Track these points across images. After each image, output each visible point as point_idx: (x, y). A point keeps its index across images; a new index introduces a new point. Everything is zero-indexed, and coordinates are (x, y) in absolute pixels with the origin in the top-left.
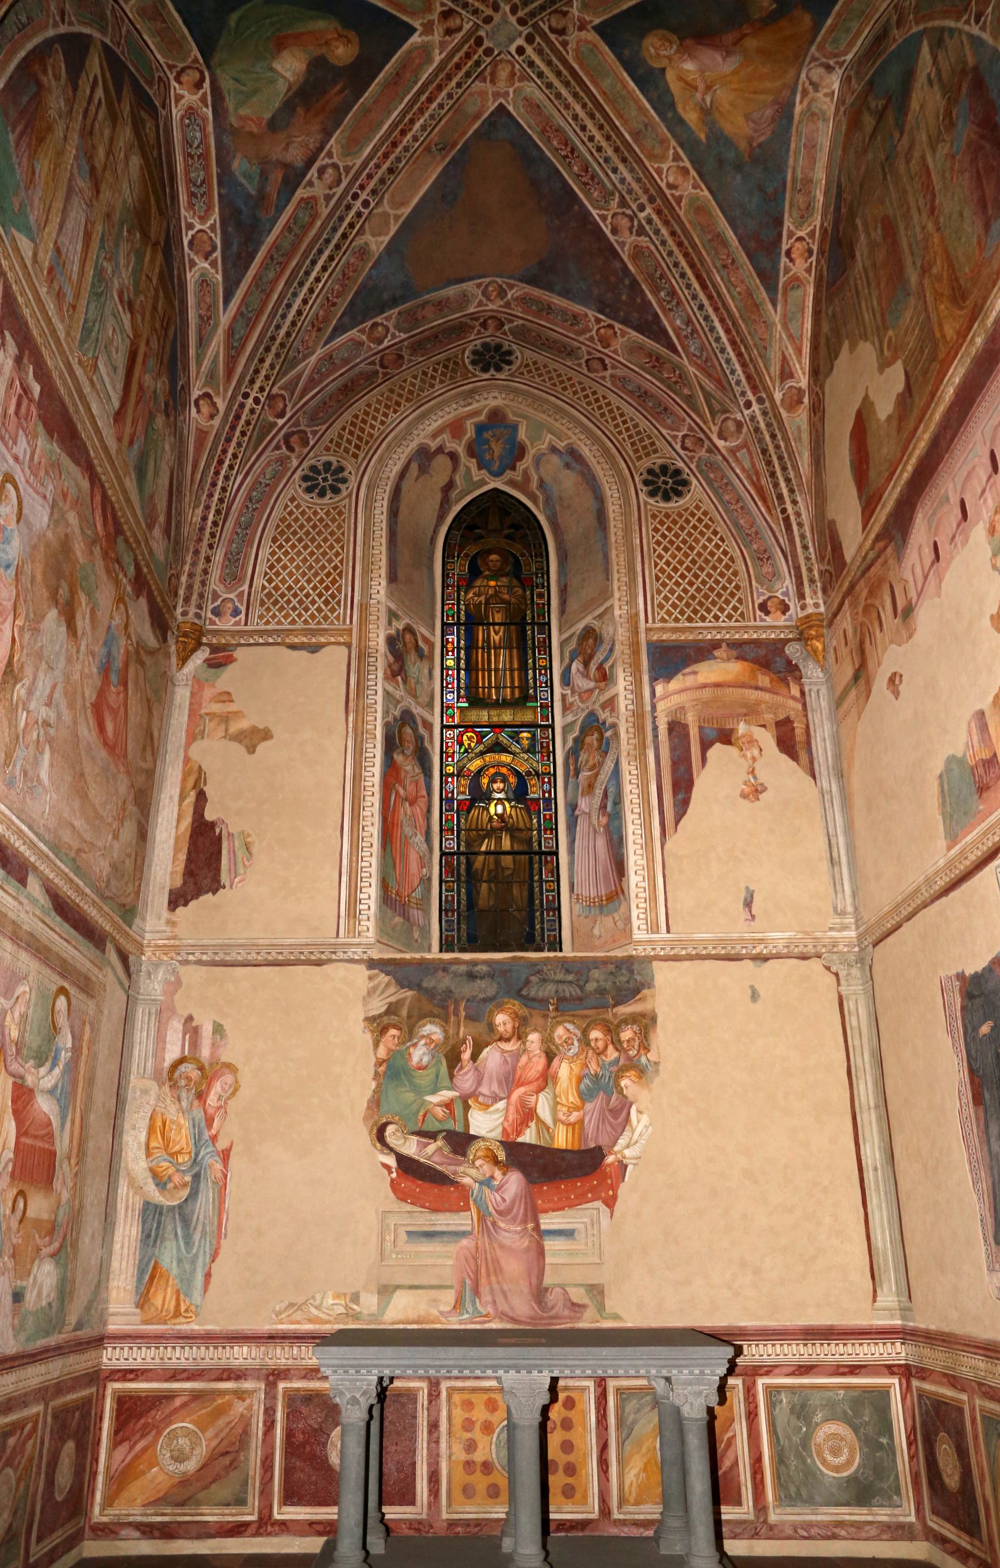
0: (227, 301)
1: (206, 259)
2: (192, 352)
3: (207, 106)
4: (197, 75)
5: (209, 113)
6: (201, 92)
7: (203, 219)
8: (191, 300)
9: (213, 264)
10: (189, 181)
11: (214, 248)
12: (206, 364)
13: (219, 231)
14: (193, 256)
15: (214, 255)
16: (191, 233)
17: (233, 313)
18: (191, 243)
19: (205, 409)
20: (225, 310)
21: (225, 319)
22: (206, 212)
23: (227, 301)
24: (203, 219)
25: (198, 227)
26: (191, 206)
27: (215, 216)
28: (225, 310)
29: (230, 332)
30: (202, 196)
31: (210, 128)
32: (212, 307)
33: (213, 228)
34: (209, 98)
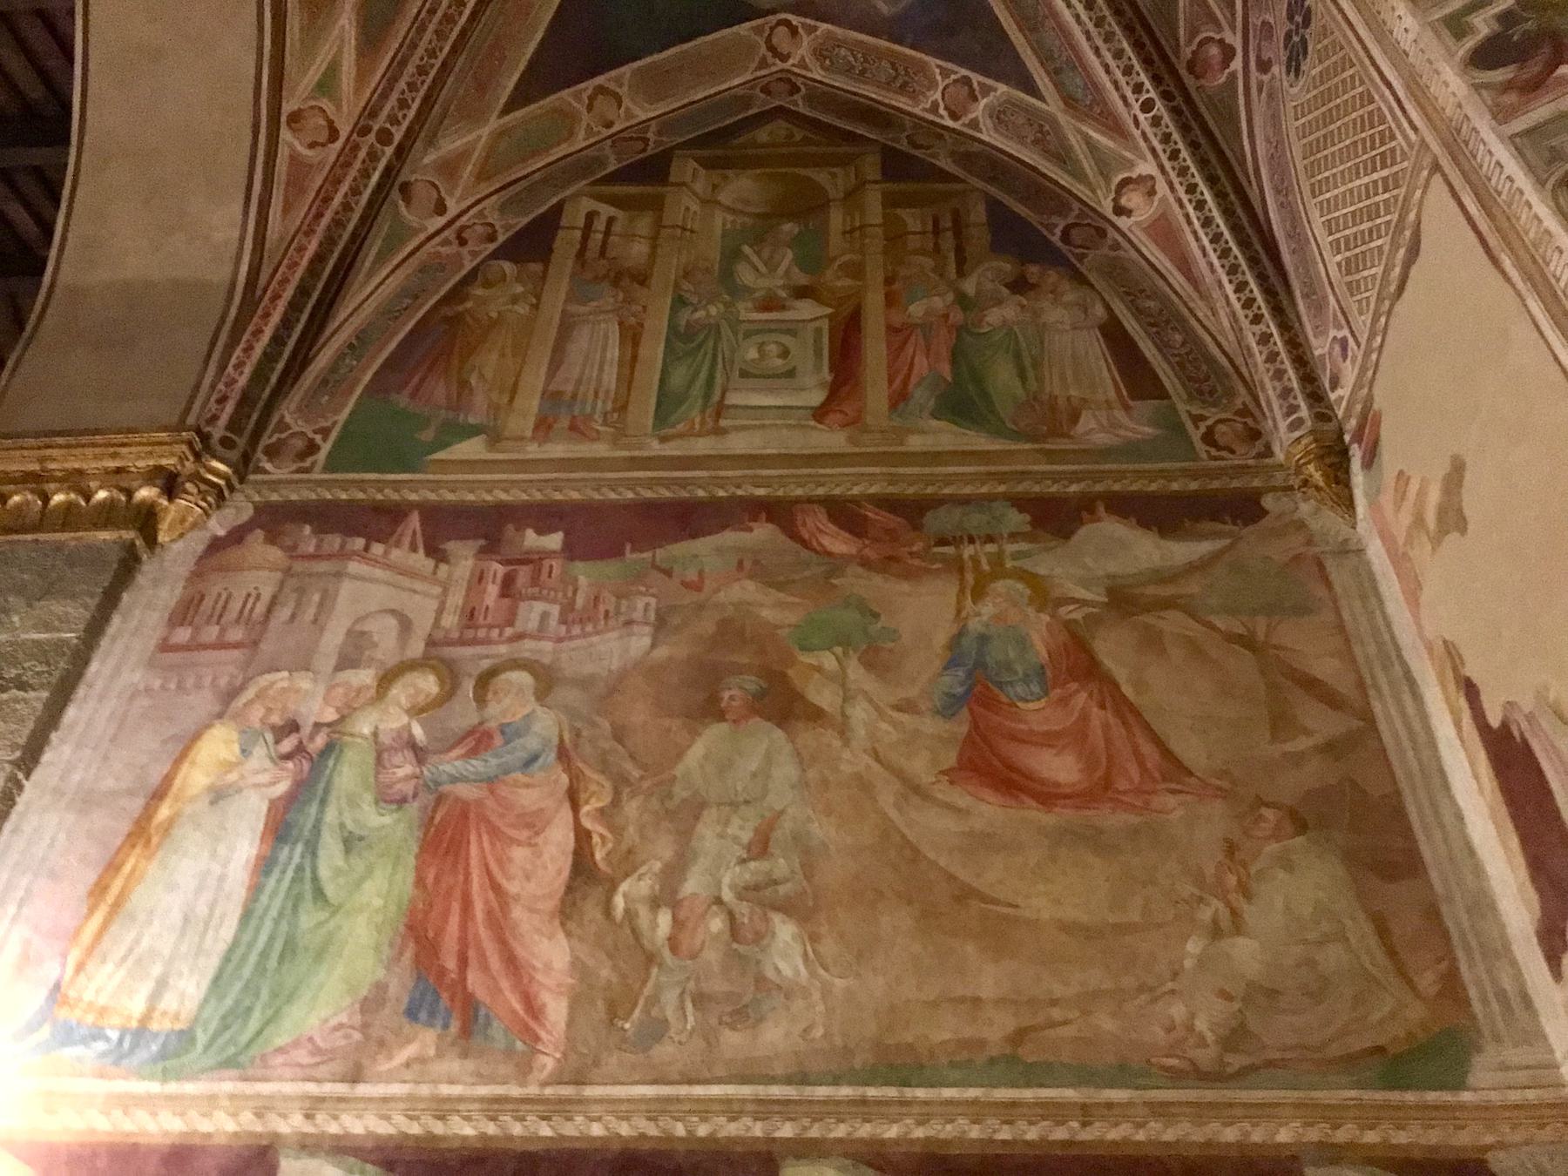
0: (1033, 90)
1: (975, 99)
2: (1065, 180)
3: (815, 28)
4: (782, 29)
5: (824, 26)
6: (800, 30)
7: (933, 84)
8: (1012, 148)
9: (987, 90)
10: (887, 85)
11: (966, 81)
12: (1088, 166)
13: (950, 65)
14: (966, 120)
15: (975, 85)
16: (942, 111)
17: (1050, 85)
18: (954, 116)
19: (1132, 199)
20: (1041, 98)
21: (1052, 105)
22: (925, 76)
23: (1033, 90)
24: (933, 84)
25: (938, 96)
26: (914, 96)
27: (933, 62)
28: (1041, 98)
29: (1070, 102)
30: (907, 73)
31: (839, 31)
32: (1032, 115)
33: (945, 73)
34: (808, 21)
